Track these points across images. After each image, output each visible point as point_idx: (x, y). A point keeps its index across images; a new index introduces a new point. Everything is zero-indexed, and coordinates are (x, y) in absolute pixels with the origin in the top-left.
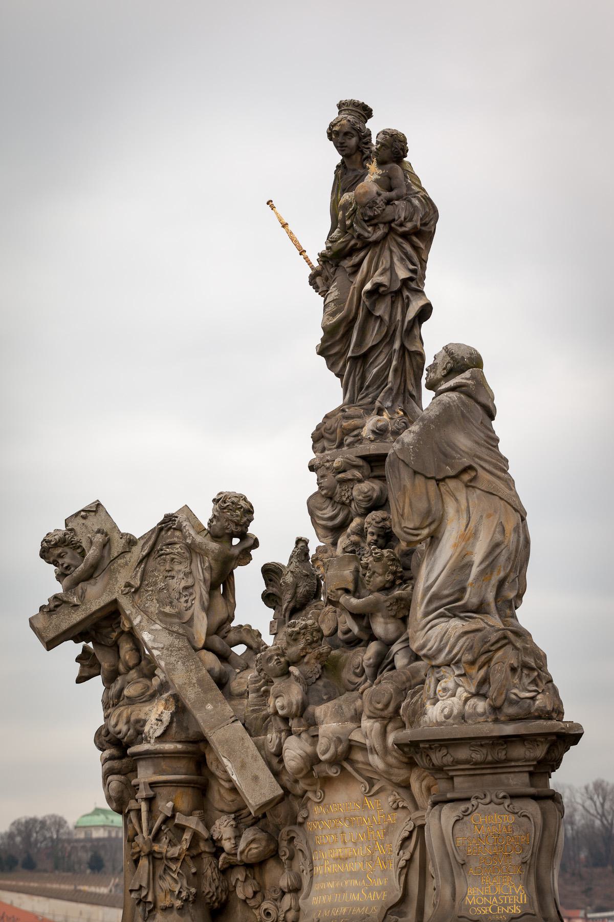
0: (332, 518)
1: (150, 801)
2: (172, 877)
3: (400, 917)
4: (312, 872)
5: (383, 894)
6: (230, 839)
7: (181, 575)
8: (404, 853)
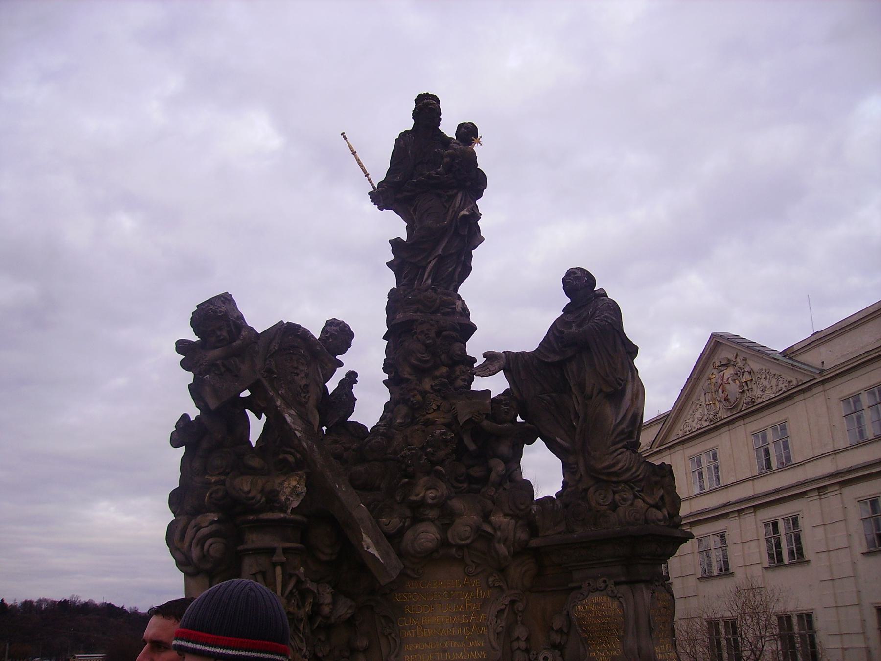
0: (427, 362)
1: (282, 564)
2: (298, 635)
6: (329, 604)
7: (303, 375)
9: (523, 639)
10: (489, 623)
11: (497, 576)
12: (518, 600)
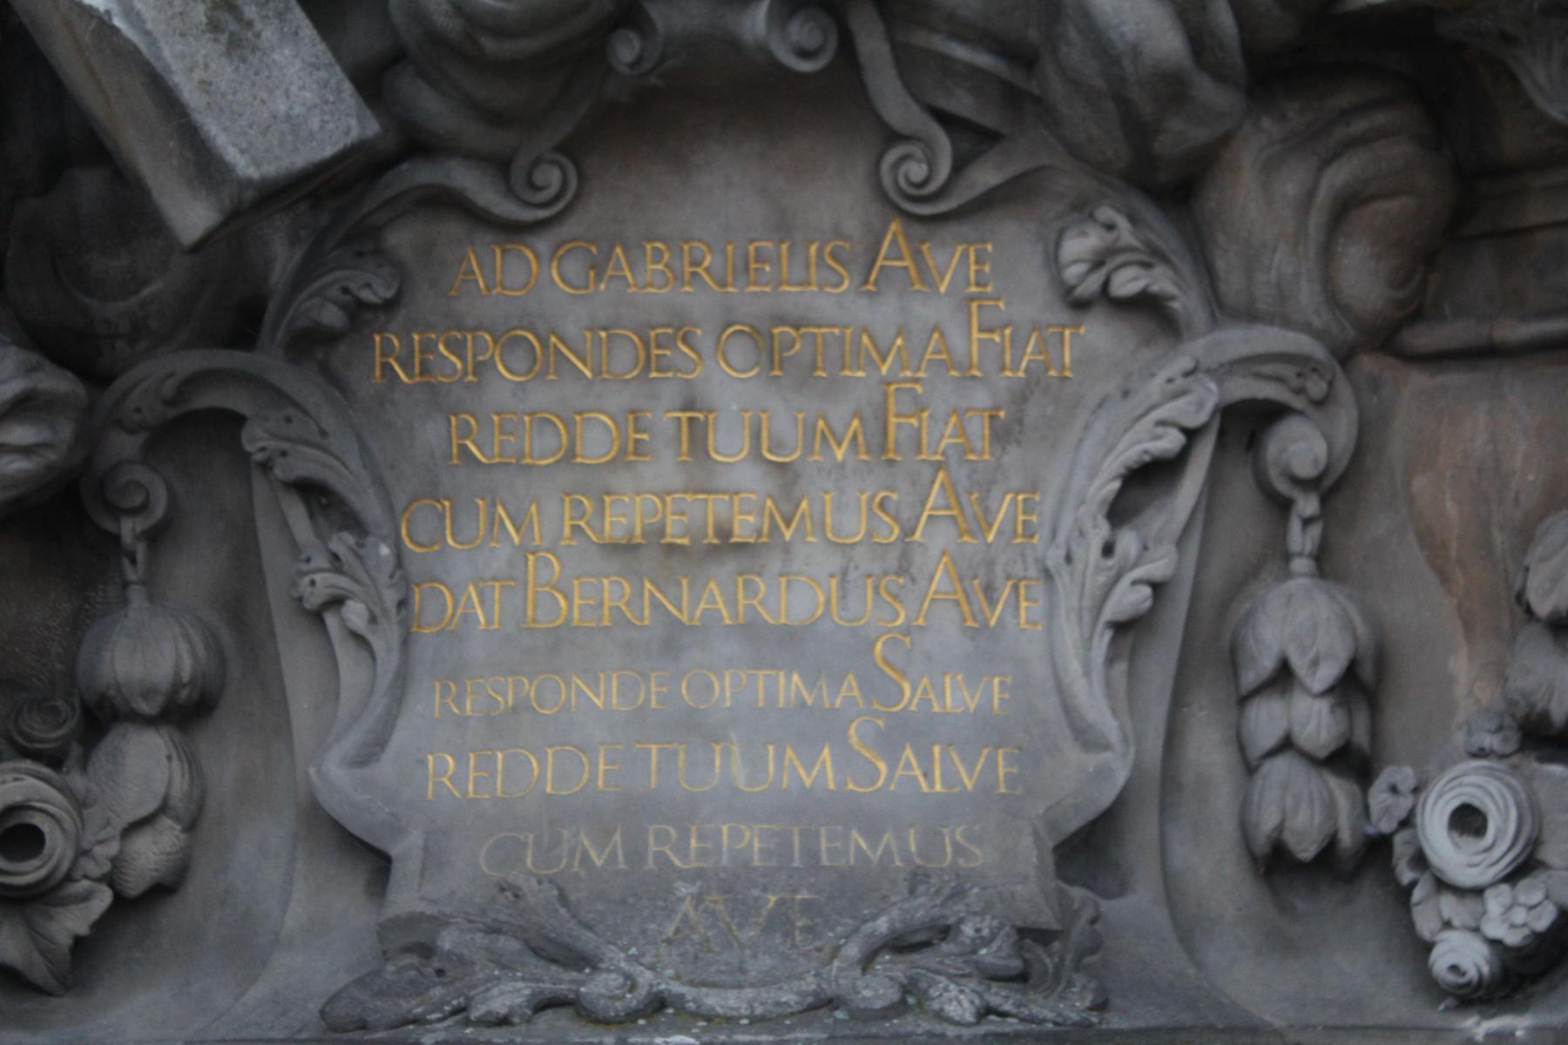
3: (1108, 895)
4: (404, 612)
5: (991, 764)
8: (1145, 548)
9: (1328, 673)
10: (1055, 557)
11: (1123, 223)
12: (1297, 403)
